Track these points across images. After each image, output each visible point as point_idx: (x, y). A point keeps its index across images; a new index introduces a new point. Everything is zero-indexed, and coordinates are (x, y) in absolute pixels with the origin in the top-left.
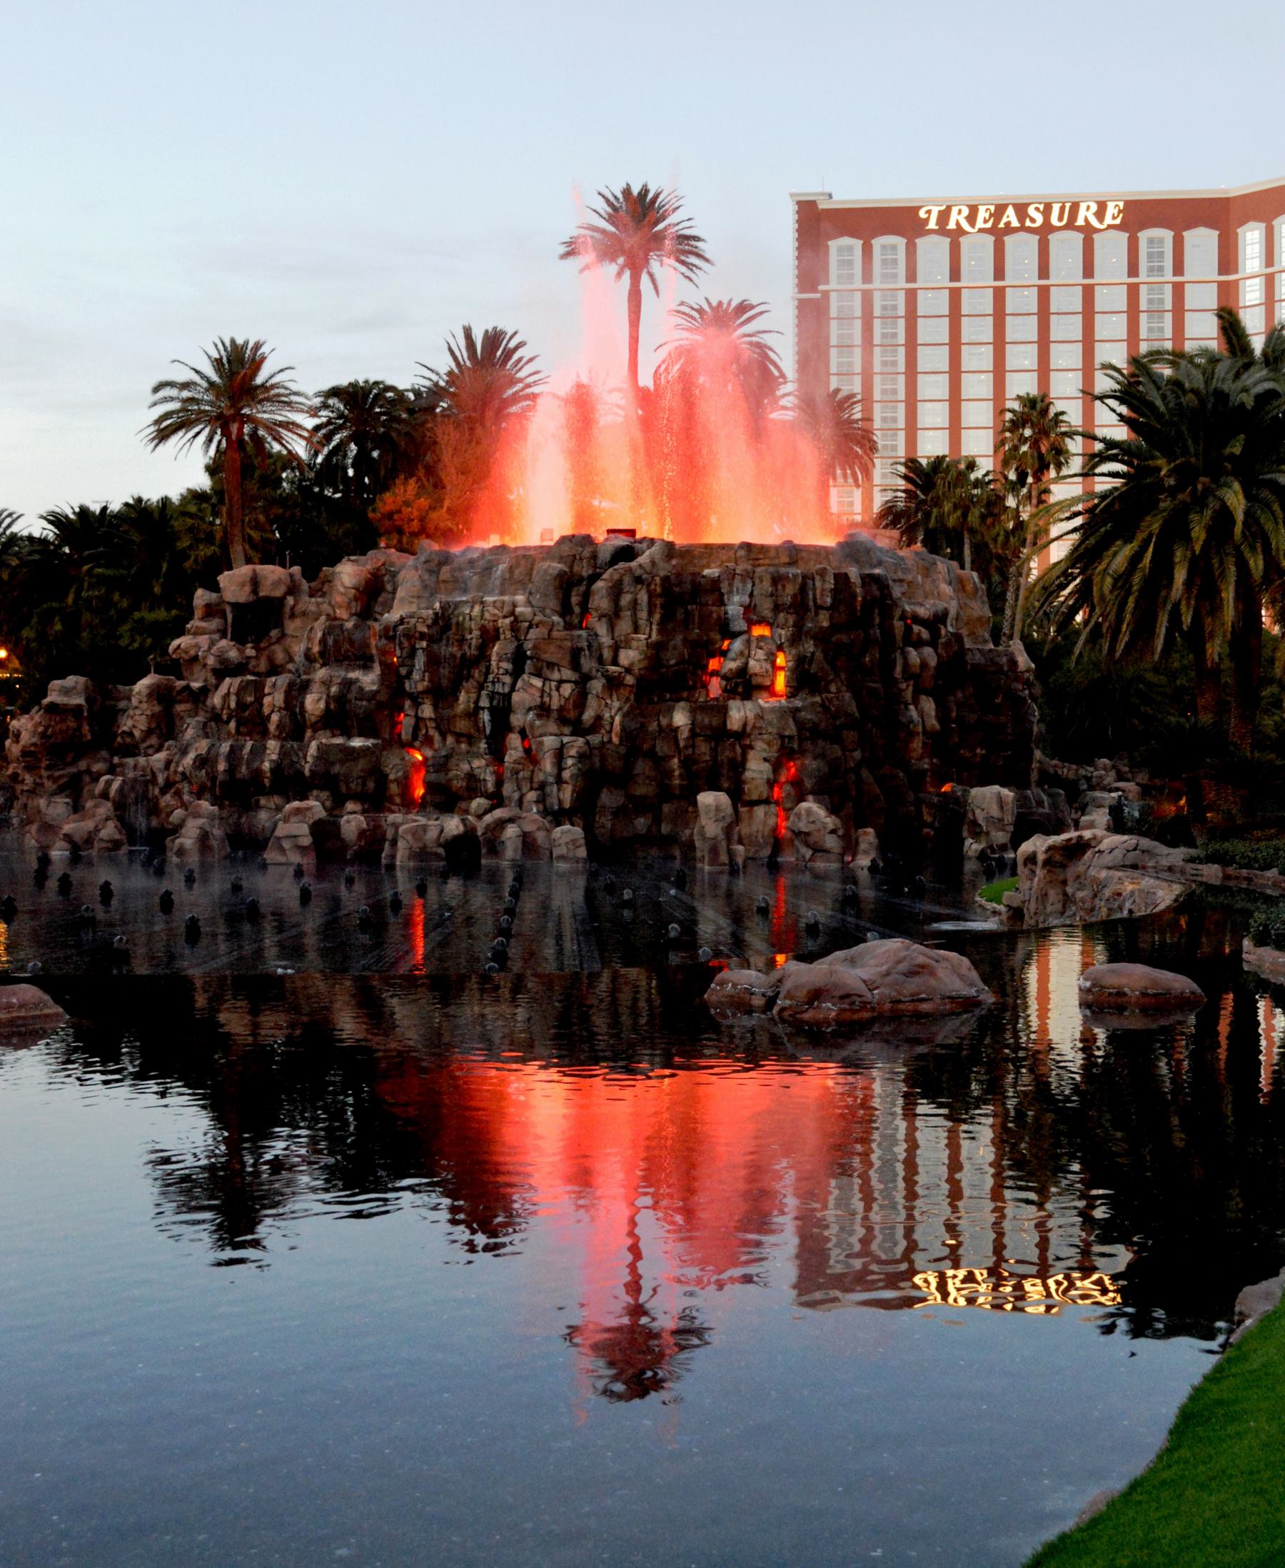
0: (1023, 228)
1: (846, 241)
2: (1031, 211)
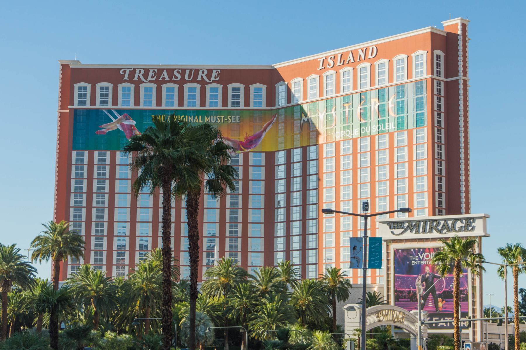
0: (171, 81)
1: (83, 84)
2: (175, 72)
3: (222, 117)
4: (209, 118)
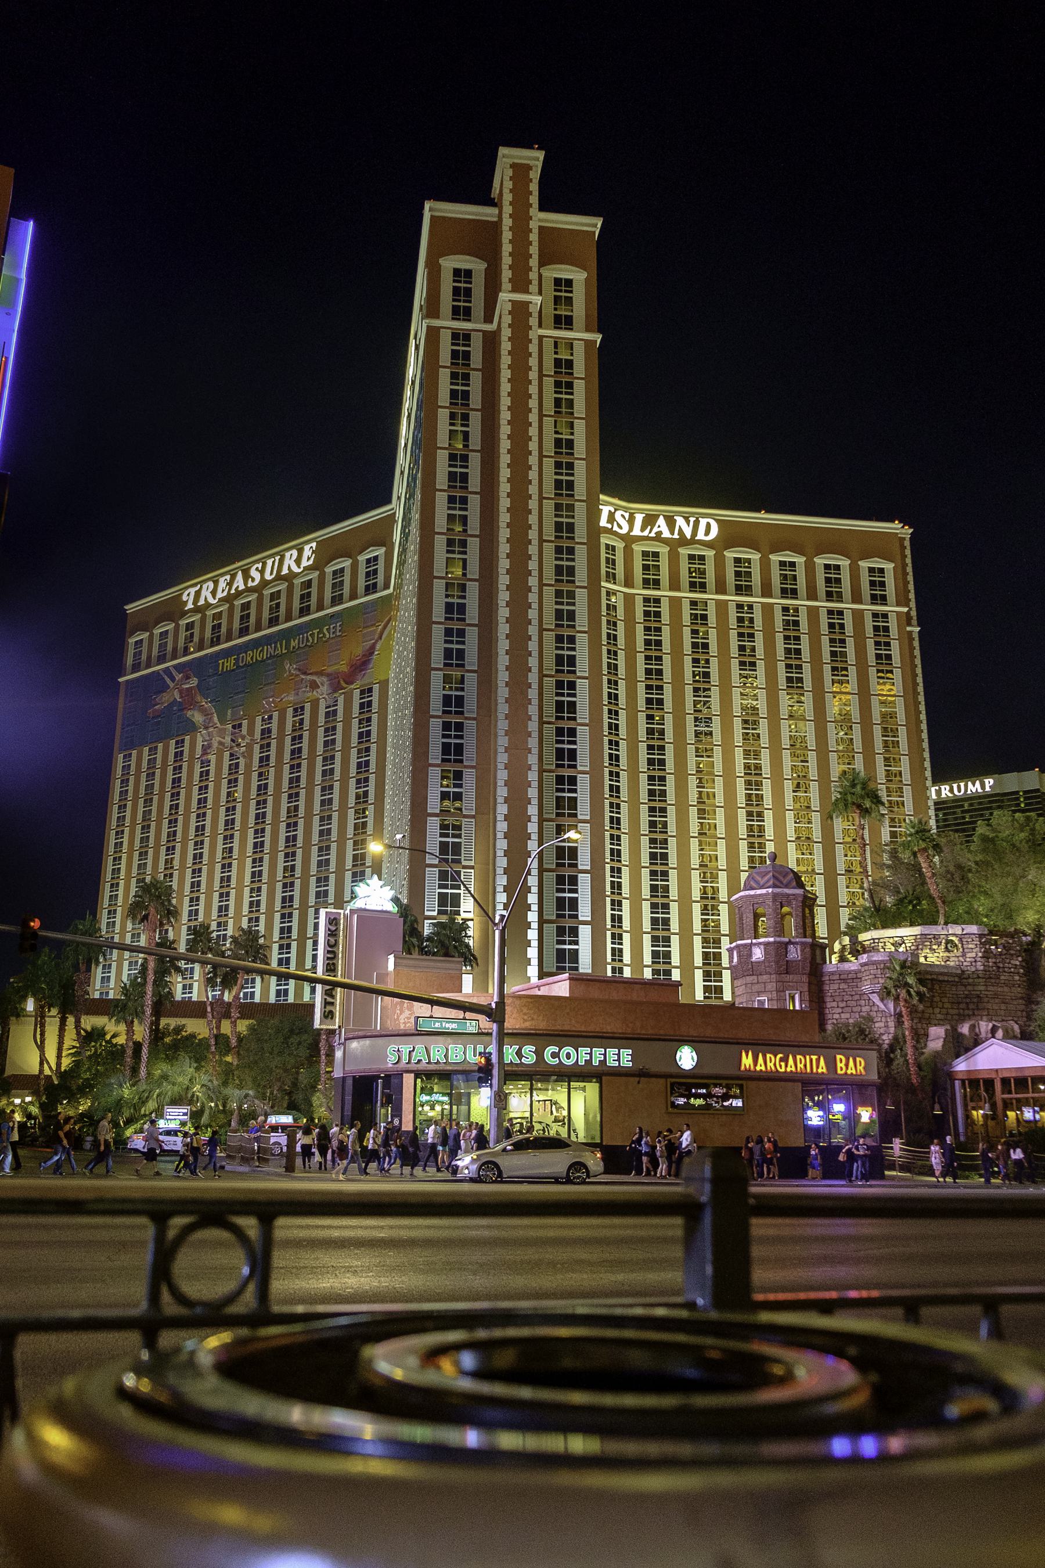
3: (316, 631)
4: (297, 641)
